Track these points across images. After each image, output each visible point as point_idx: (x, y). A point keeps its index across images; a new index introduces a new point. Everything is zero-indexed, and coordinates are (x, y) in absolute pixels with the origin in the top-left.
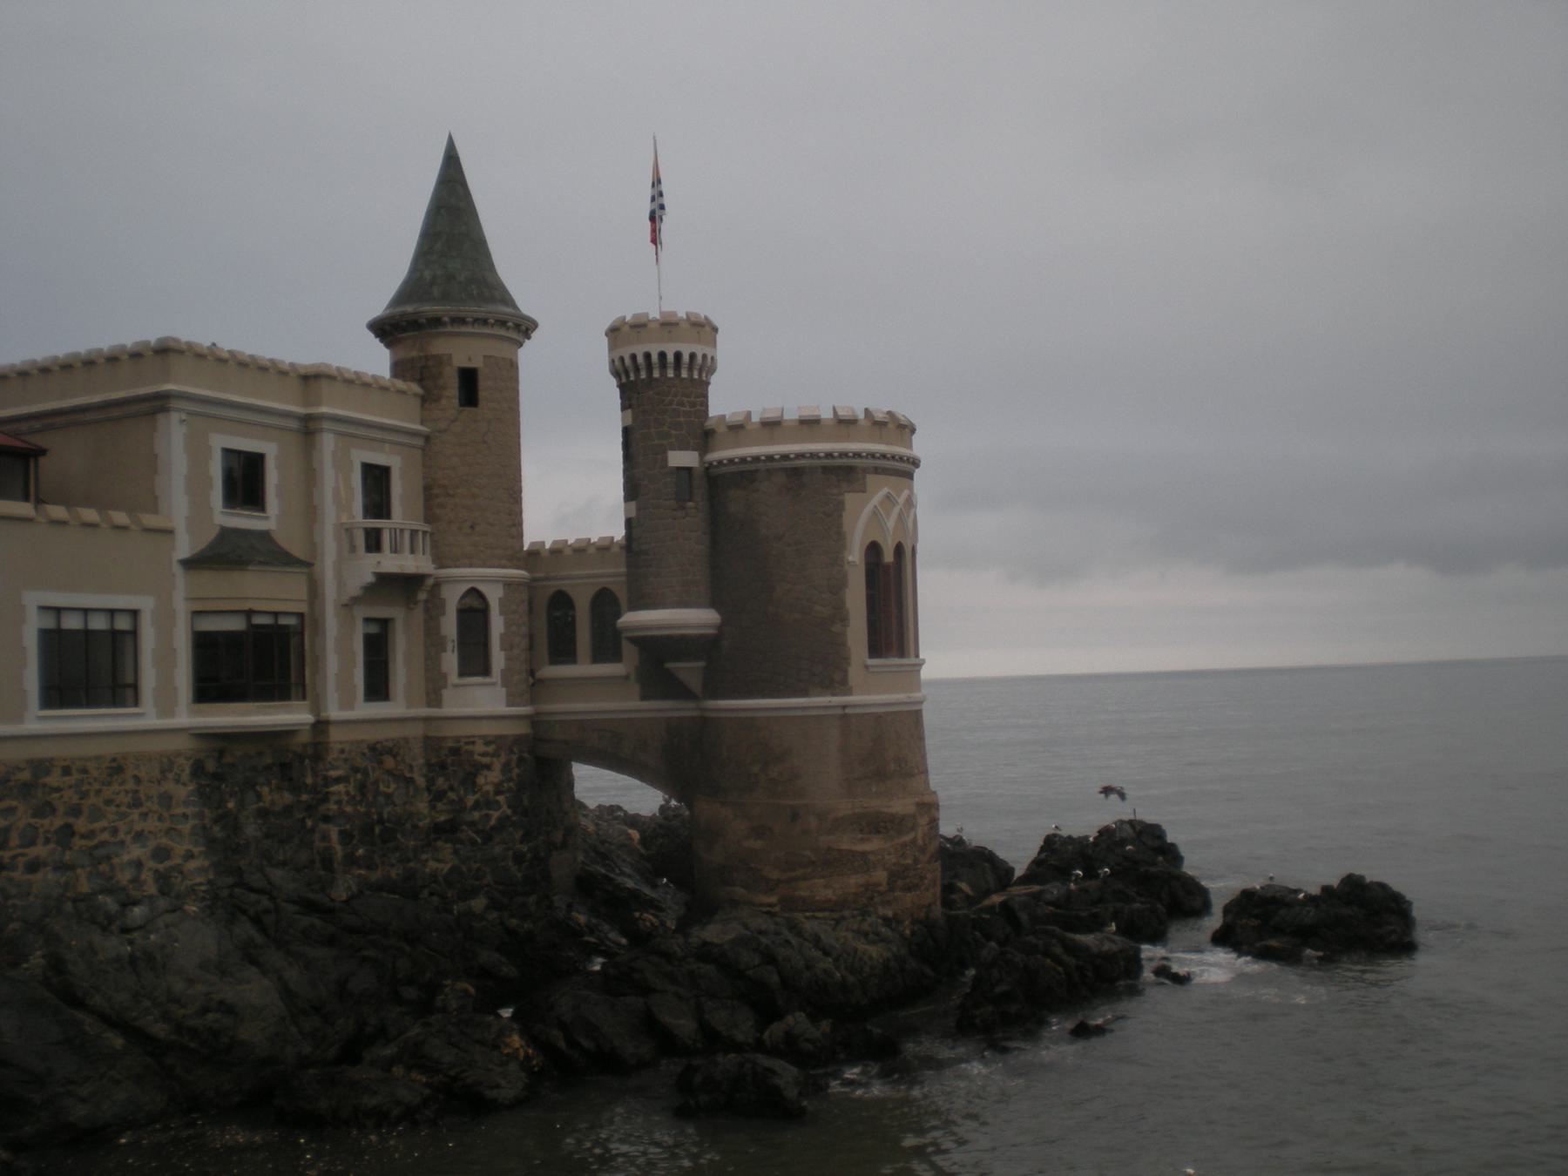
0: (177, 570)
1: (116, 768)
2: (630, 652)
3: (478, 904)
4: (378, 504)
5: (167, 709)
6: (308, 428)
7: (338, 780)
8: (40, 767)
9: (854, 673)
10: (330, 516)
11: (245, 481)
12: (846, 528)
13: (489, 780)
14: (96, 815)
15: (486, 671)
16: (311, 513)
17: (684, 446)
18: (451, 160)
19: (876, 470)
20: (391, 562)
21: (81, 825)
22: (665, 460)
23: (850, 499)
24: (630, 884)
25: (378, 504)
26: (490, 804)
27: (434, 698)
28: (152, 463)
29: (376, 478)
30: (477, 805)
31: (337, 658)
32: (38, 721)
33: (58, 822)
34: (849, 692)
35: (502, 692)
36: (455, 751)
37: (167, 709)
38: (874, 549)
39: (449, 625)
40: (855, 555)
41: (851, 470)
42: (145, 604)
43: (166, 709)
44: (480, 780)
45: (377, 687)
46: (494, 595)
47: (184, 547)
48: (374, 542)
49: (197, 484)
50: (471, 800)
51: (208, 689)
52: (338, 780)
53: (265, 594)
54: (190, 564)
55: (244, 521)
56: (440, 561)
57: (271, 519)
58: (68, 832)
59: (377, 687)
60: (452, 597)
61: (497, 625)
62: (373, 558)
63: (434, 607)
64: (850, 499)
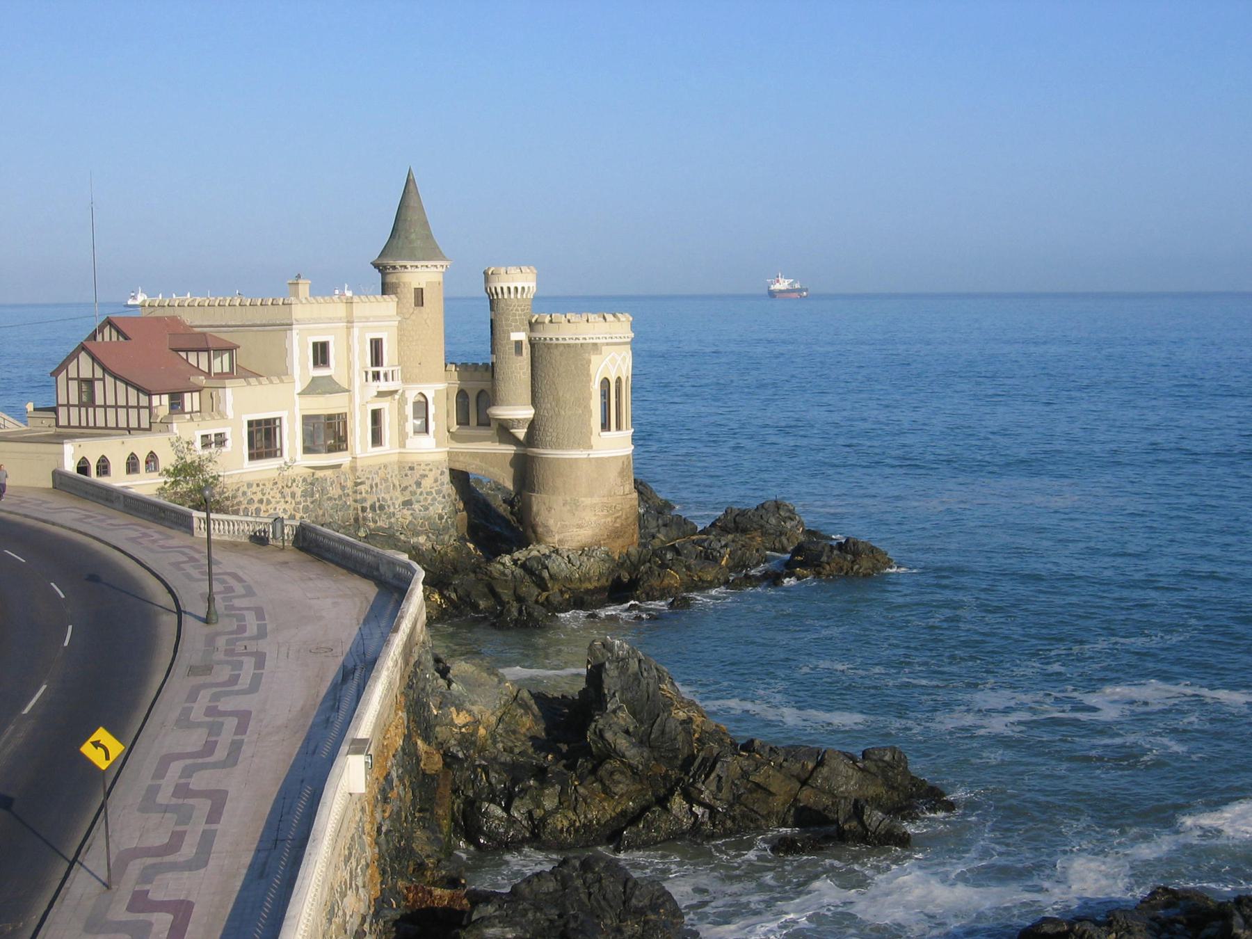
0: (297, 397)
2: (494, 425)
3: (422, 539)
4: (377, 359)
7: (361, 483)
8: (249, 485)
9: (594, 439)
10: (357, 366)
11: (321, 354)
12: (592, 371)
13: (427, 483)
14: (269, 502)
15: (427, 431)
16: (350, 366)
17: (518, 330)
18: (409, 182)
19: (607, 344)
20: (383, 385)
21: (263, 507)
22: (509, 337)
23: (594, 358)
24: (497, 529)
25: (377, 359)
26: (429, 493)
27: (402, 444)
28: (284, 354)
29: (376, 345)
30: (421, 494)
31: (359, 430)
33: (256, 505)
34: (591, 447)
35: (433, 441)
36: (411, 468)
38: (605, 383)
39: (409, 410)
41: (595, 345)
42: (284, 414)
44: (423, 482)
45: (377, 439)
47: (299, 388)
48: (376, 376)
50: (419, 491)
51: (307, 450)
52: (361, 483)
56: (405, 380)
58: (258, 511)
59: (377, 439)
60: (412, 396)
62: (376, 383)
63: (402, 402)
64: (594, 358)
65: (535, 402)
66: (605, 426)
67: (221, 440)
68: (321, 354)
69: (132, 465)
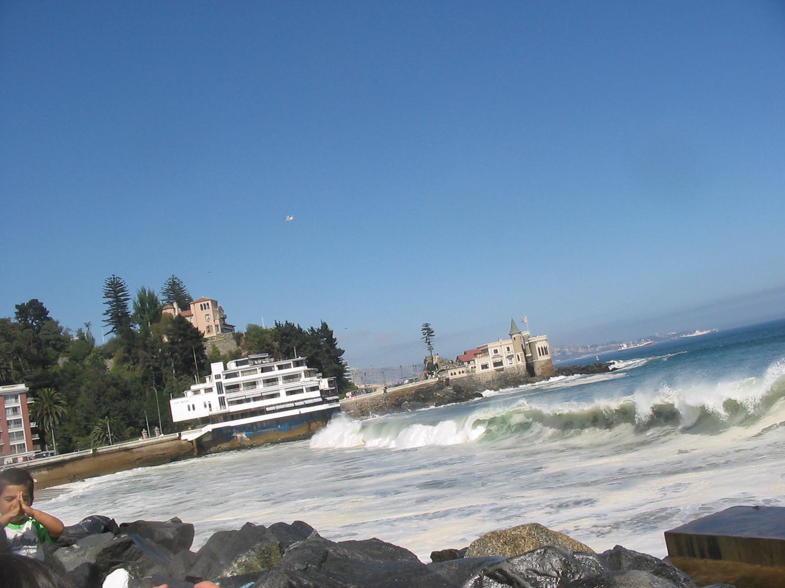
1: (488, 373)
5: (491, 368)
6: (501, 346)
11: (496, 351)
23: (536, 344)
27: (517, 363)
32: (481, 370)
37: (491, 368)
40: (537, 349)
43: (492, 368)
46: (519, 355)
47: (491, 357)
49: (492, 353)
53: (498, 360)
54: (492, 358)
55: (497, 354)
57: (499, 353)
61: (520, 357)
65: (531, 353)
66: (540, 355)
67: (475, 367)
68: (496, 351)
69: (460, 373)
